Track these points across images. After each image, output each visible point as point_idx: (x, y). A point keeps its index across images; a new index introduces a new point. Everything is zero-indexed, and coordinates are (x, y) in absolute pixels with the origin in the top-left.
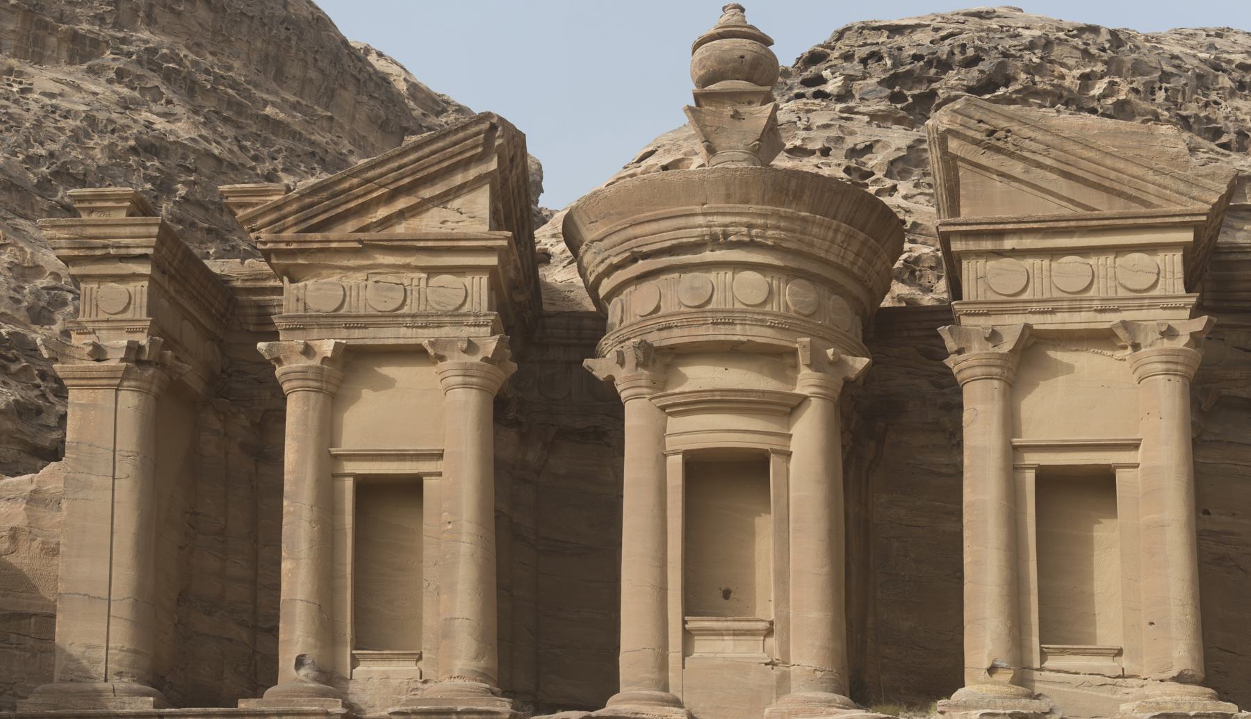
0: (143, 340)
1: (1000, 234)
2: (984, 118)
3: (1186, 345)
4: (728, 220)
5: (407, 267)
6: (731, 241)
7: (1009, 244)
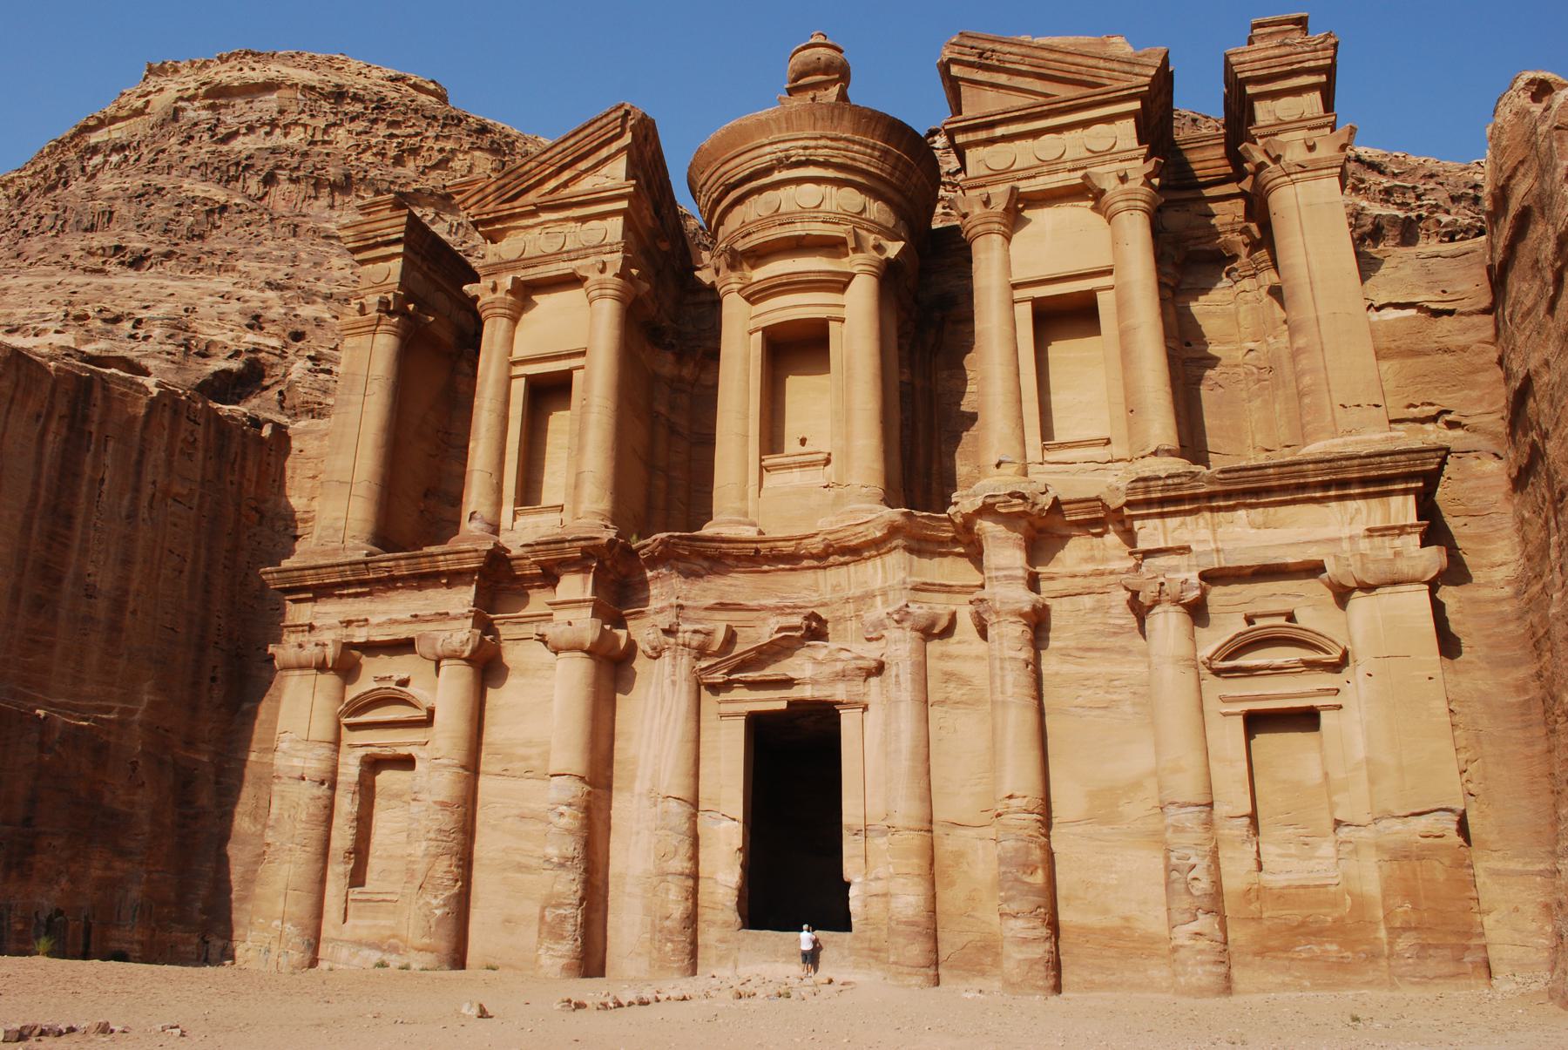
0: (390, 297)
1: (992, 125)
2: (975, 44)
3: (1142, 185)
4: (788, 145)
5: (567, 219)
7: (999, 131)
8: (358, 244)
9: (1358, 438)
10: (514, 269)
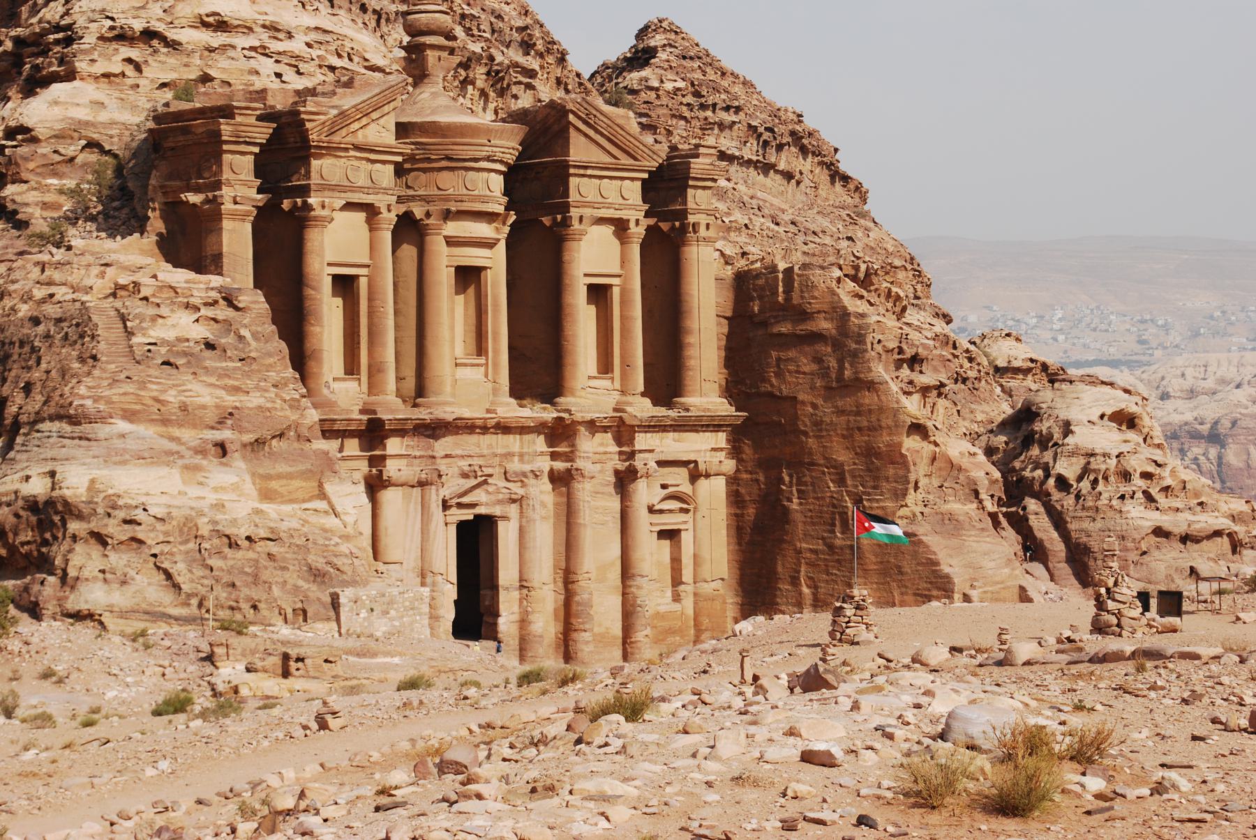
1: (586, 168)
2: (588, 107)
7: (589, 172)
8: (231, 139)
9: (710, 400)
10: (333, 190)
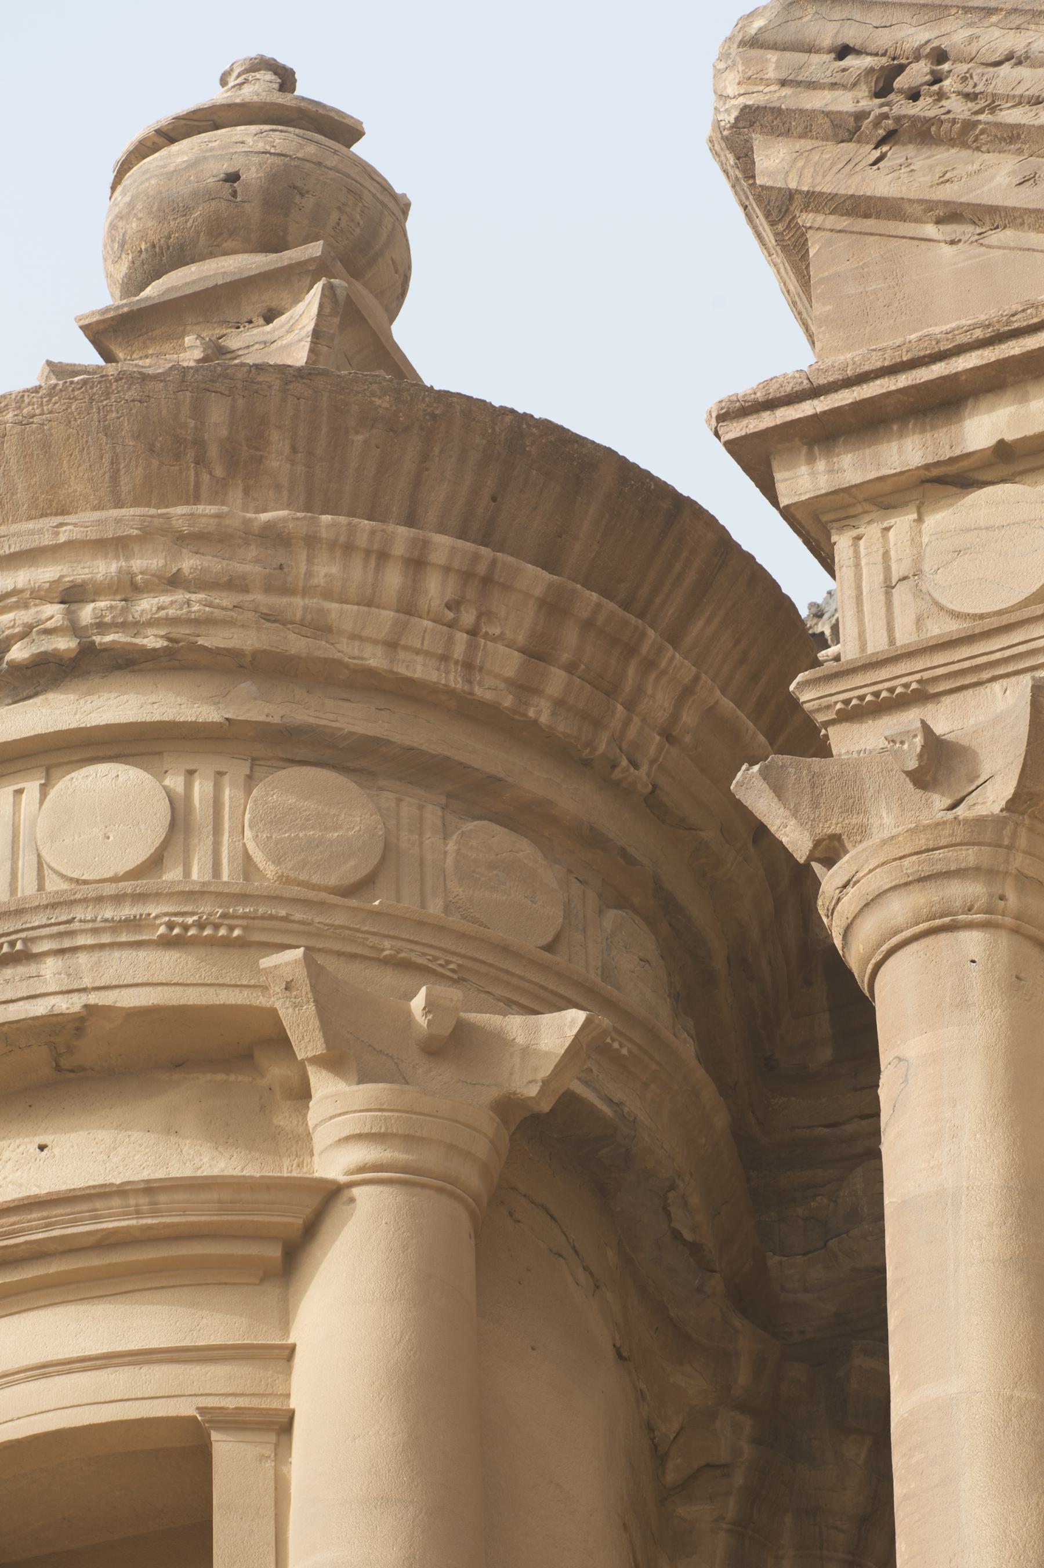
6: (16, 668)
